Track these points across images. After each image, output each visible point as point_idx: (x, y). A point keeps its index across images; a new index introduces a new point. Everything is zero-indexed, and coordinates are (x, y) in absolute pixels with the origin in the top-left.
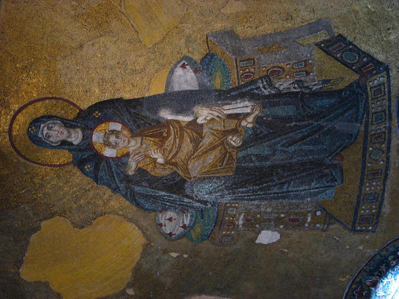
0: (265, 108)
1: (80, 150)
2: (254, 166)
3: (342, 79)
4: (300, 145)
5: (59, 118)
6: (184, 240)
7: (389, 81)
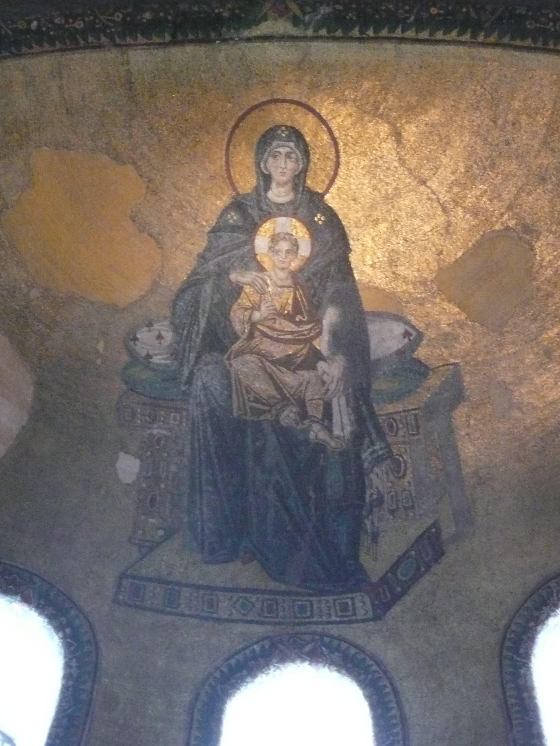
3: (375, 559)
6: (125, 358)
7: (357, 621)
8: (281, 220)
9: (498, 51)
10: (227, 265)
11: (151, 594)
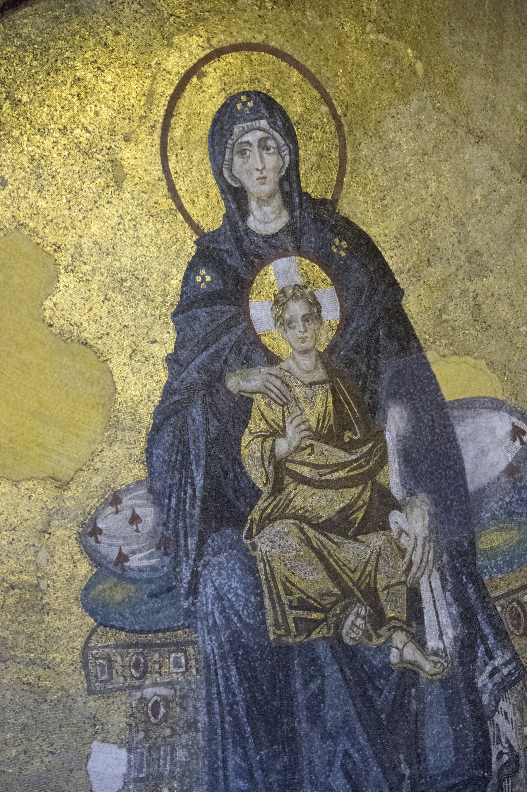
0: (442, 687)
1: (239, 241)
2: (295, 692)
5: (297, 155)
8: (282, 263)
10: (217, 366)
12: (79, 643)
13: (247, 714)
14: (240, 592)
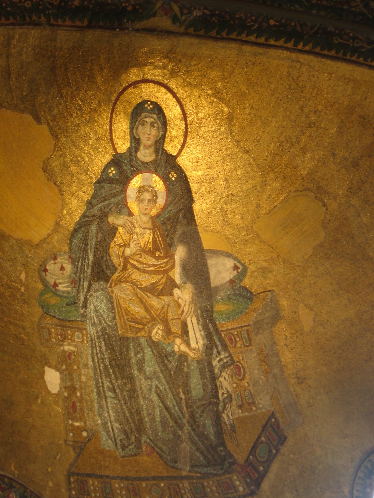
2: (131, 358)
3: (238, 445)
4: (160, 407)
6: (40, 286)
8: (147, 175)
9: (310, 58)
10: (107, 210)
11: (92, 488)
12: (36, 319)
13: (110, 364)
14: (105, 310)
